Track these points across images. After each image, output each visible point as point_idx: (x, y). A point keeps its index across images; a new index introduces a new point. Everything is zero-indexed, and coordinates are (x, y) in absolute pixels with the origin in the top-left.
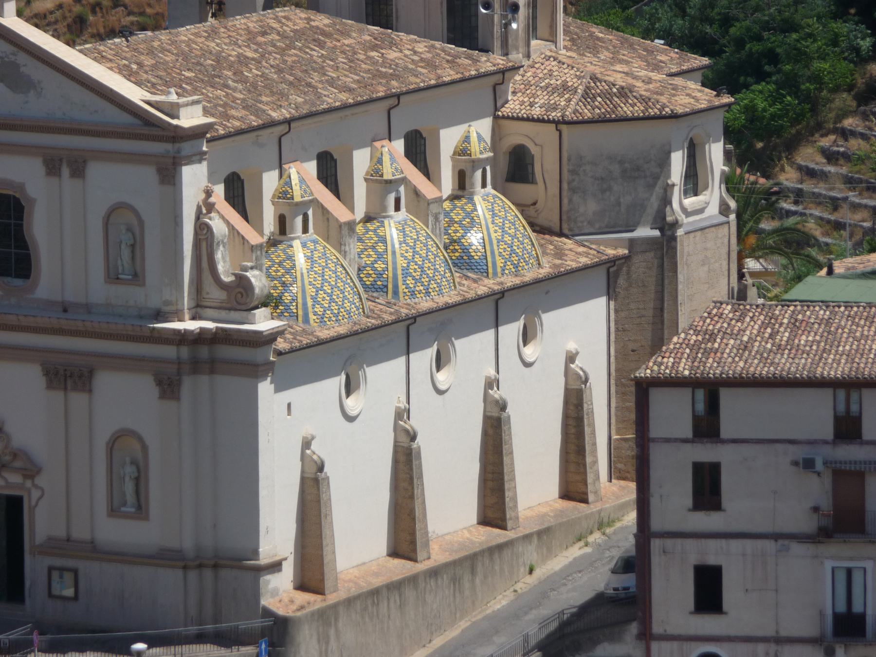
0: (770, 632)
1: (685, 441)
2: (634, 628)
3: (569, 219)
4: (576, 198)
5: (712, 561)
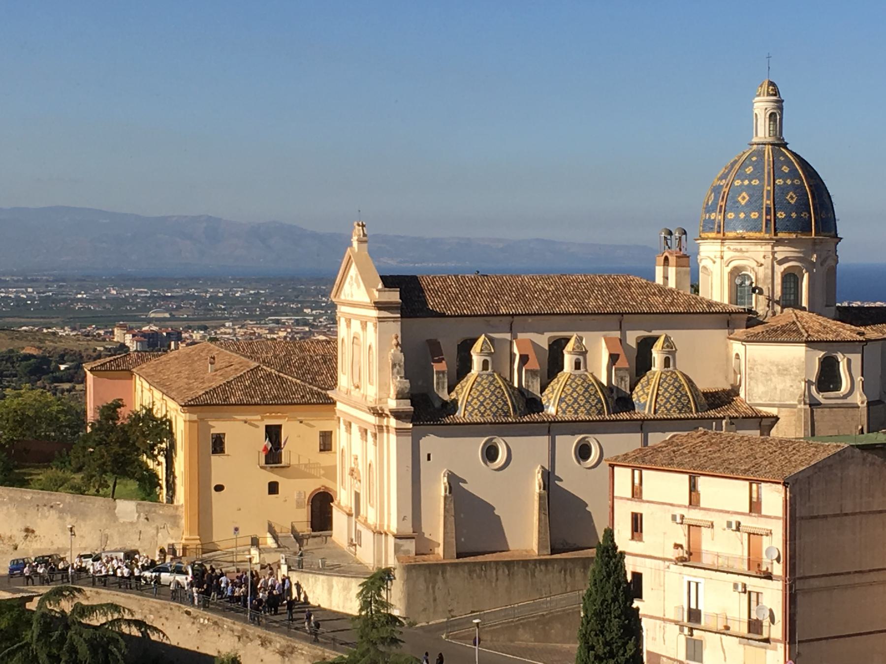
0: (661, 616)
1: (628, 499)
4: (752, 383)
5: (638, 570)
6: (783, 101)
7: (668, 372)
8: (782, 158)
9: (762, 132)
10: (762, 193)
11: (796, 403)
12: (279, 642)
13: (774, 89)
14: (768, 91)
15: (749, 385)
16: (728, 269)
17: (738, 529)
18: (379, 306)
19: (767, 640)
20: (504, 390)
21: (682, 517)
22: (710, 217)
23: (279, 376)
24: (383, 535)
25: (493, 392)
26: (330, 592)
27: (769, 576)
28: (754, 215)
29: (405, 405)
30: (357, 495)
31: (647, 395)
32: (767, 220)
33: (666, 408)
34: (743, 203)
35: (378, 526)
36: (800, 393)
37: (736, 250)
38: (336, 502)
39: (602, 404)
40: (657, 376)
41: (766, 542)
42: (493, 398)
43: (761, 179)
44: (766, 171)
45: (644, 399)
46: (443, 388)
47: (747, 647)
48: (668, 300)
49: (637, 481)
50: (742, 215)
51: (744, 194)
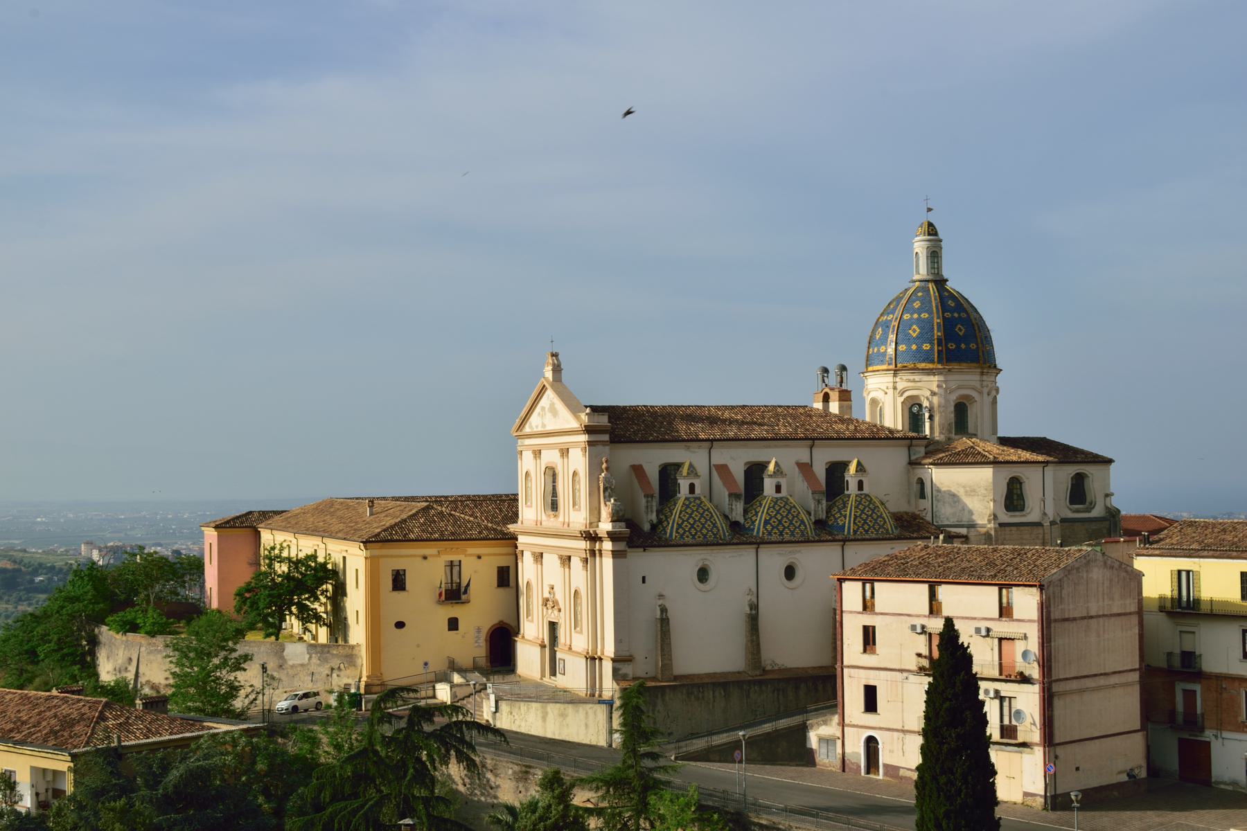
0: (900, 728)
1: (859, 613)
2: (836, 719)
3: (936, 515)
5: (872, 683)
6: (941, 241)
7: (861, 494)
8: (946, 294)
9: (923, 271)
10: (933, 325)
11: (986, 522)
12: (511, 768)
13: (931, 230)
14: (928, 231)
15: (936, 506)
16: (902, 399)
17: (988, 636)
18: (589, 430)
19: (1024, 745)
20: (712, 511)
21: (923, 627)
22: (879, 350)
23: (451, 515)
24: (597, 661)
25: (702, 515)
26: (544, 718)
27: (1024, 679)
28: (926, 347)
29: (620, 527)
30: (553, 626)
31: (845, 517)
32: (938, 350)
33: (864, 529)
34: (914, 335)
35: (590, 651)
36: (988, 513)
37: (909, 381)
38: (520, 636)
39: (805, 526)
40: (853, 498)
41: (1020, 647)
42: (703, 520)
43: (930, 313)
44: (934, 305)
45: (842, 520)
46: (652, 511)
47: (999, 753)
48: (851, 427)
49: (868, 594)
50: (914, 347)
51: (914, 327)
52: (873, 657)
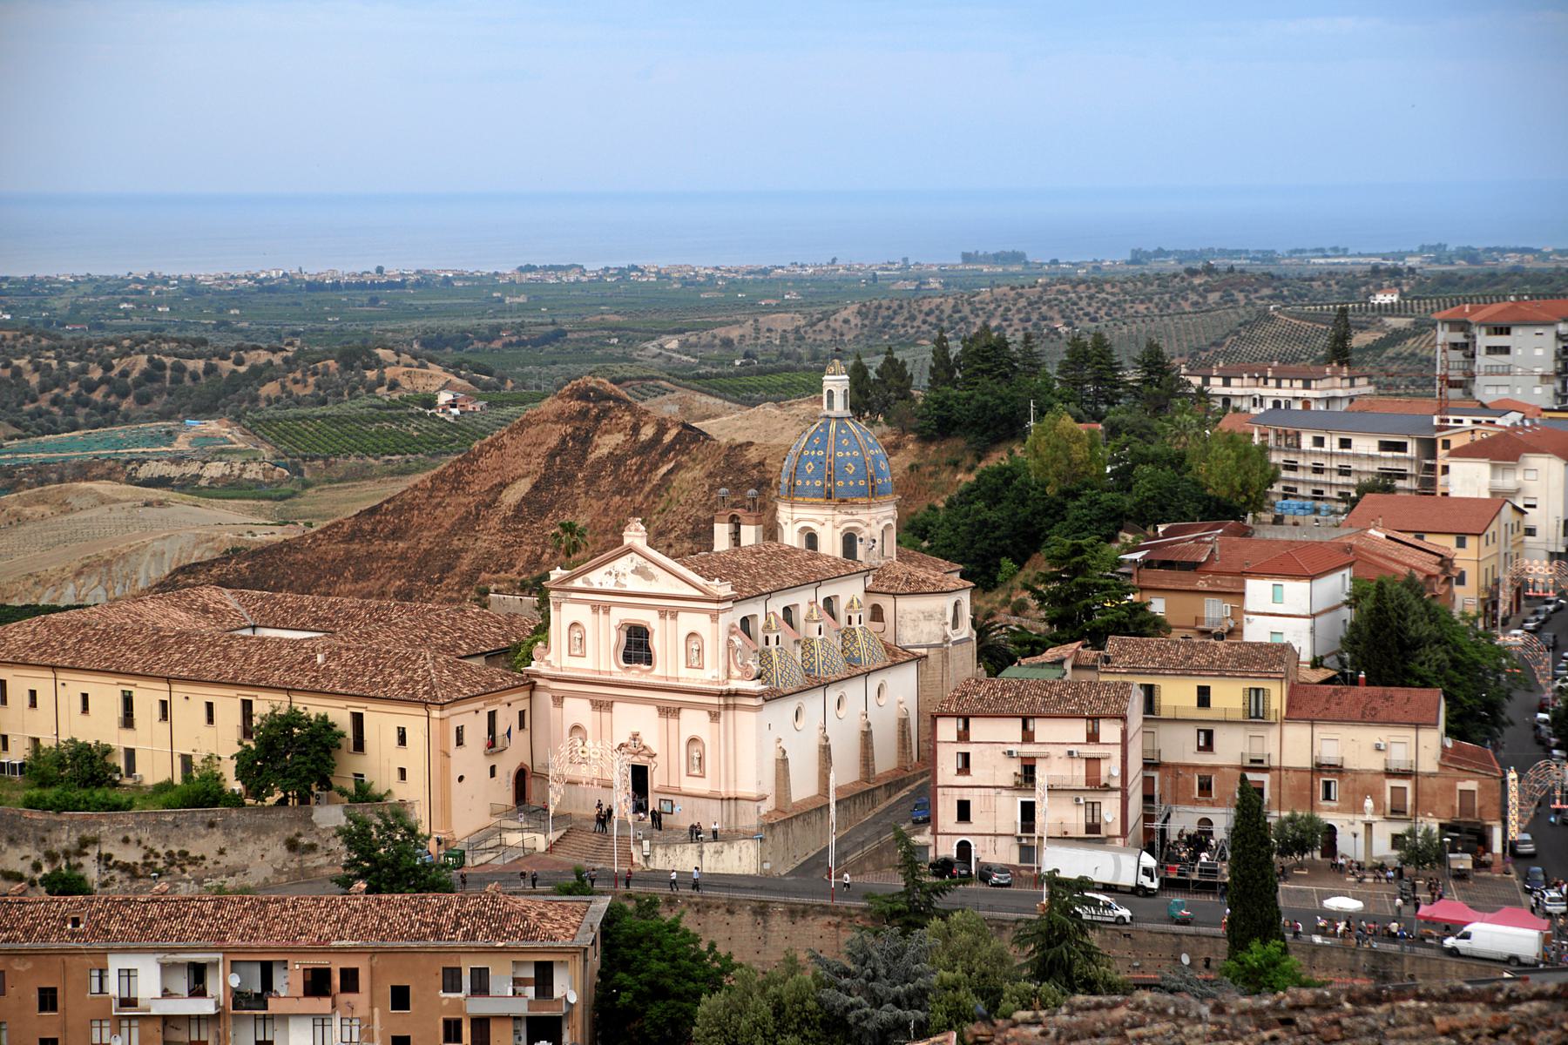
2: (929, 829)
5: (966, 798)
37: (847, 513)
41: (1104, 765)
50: (851, 483)
52: (967, 777)
